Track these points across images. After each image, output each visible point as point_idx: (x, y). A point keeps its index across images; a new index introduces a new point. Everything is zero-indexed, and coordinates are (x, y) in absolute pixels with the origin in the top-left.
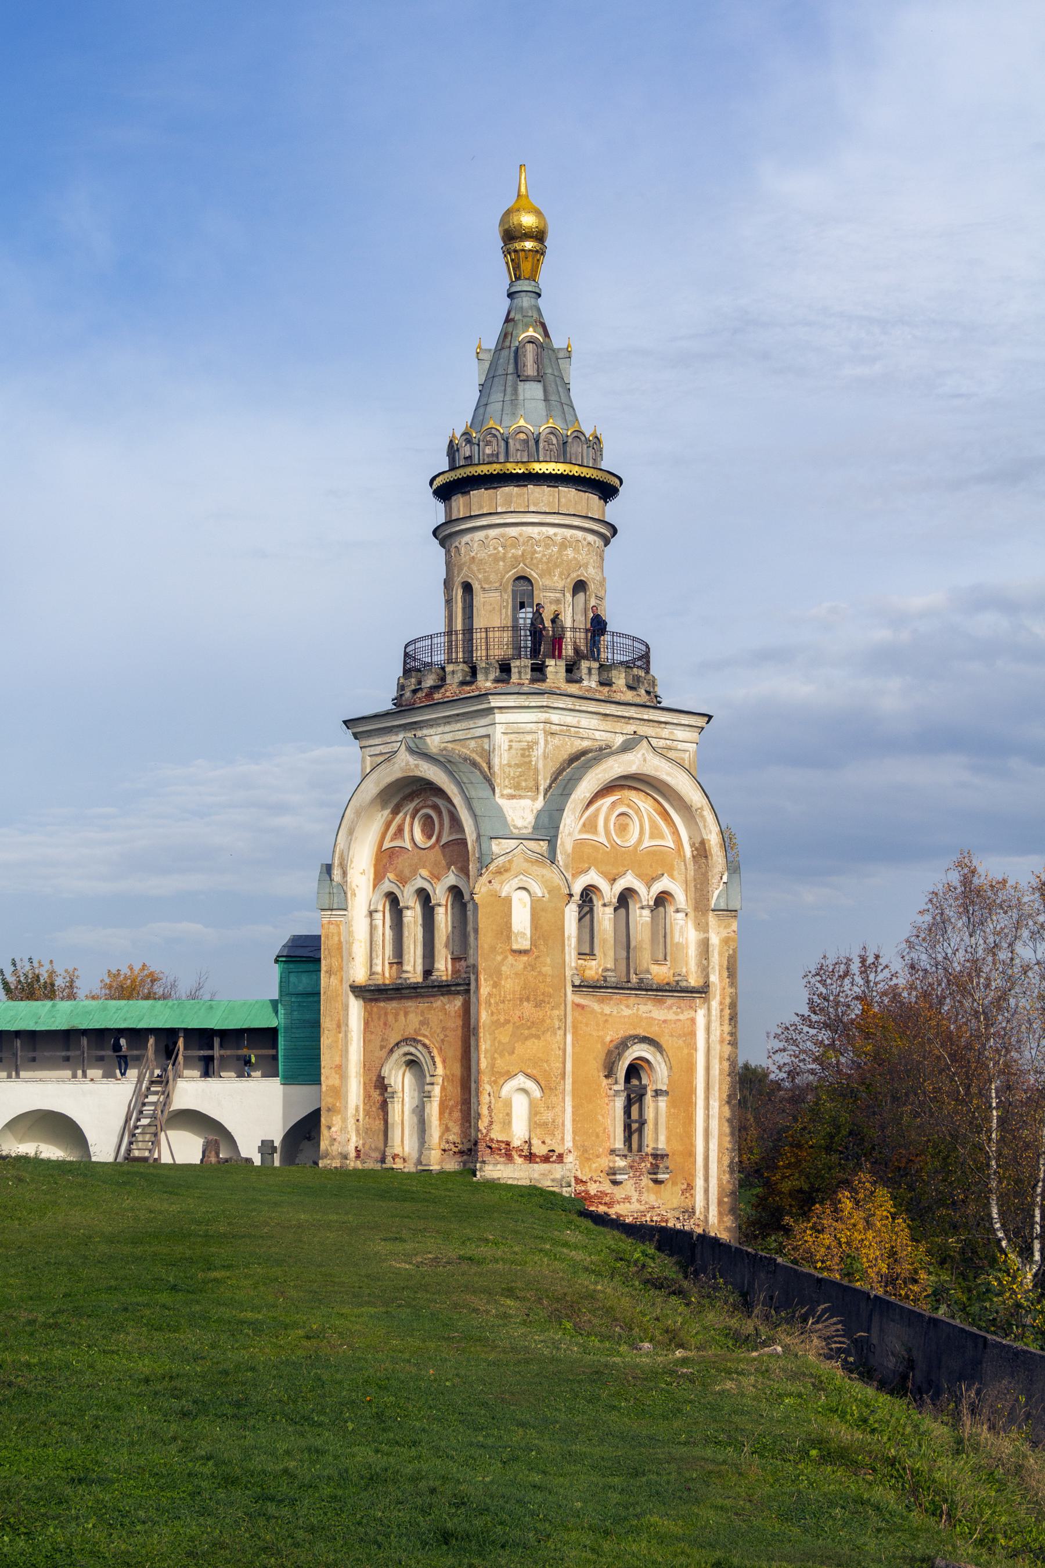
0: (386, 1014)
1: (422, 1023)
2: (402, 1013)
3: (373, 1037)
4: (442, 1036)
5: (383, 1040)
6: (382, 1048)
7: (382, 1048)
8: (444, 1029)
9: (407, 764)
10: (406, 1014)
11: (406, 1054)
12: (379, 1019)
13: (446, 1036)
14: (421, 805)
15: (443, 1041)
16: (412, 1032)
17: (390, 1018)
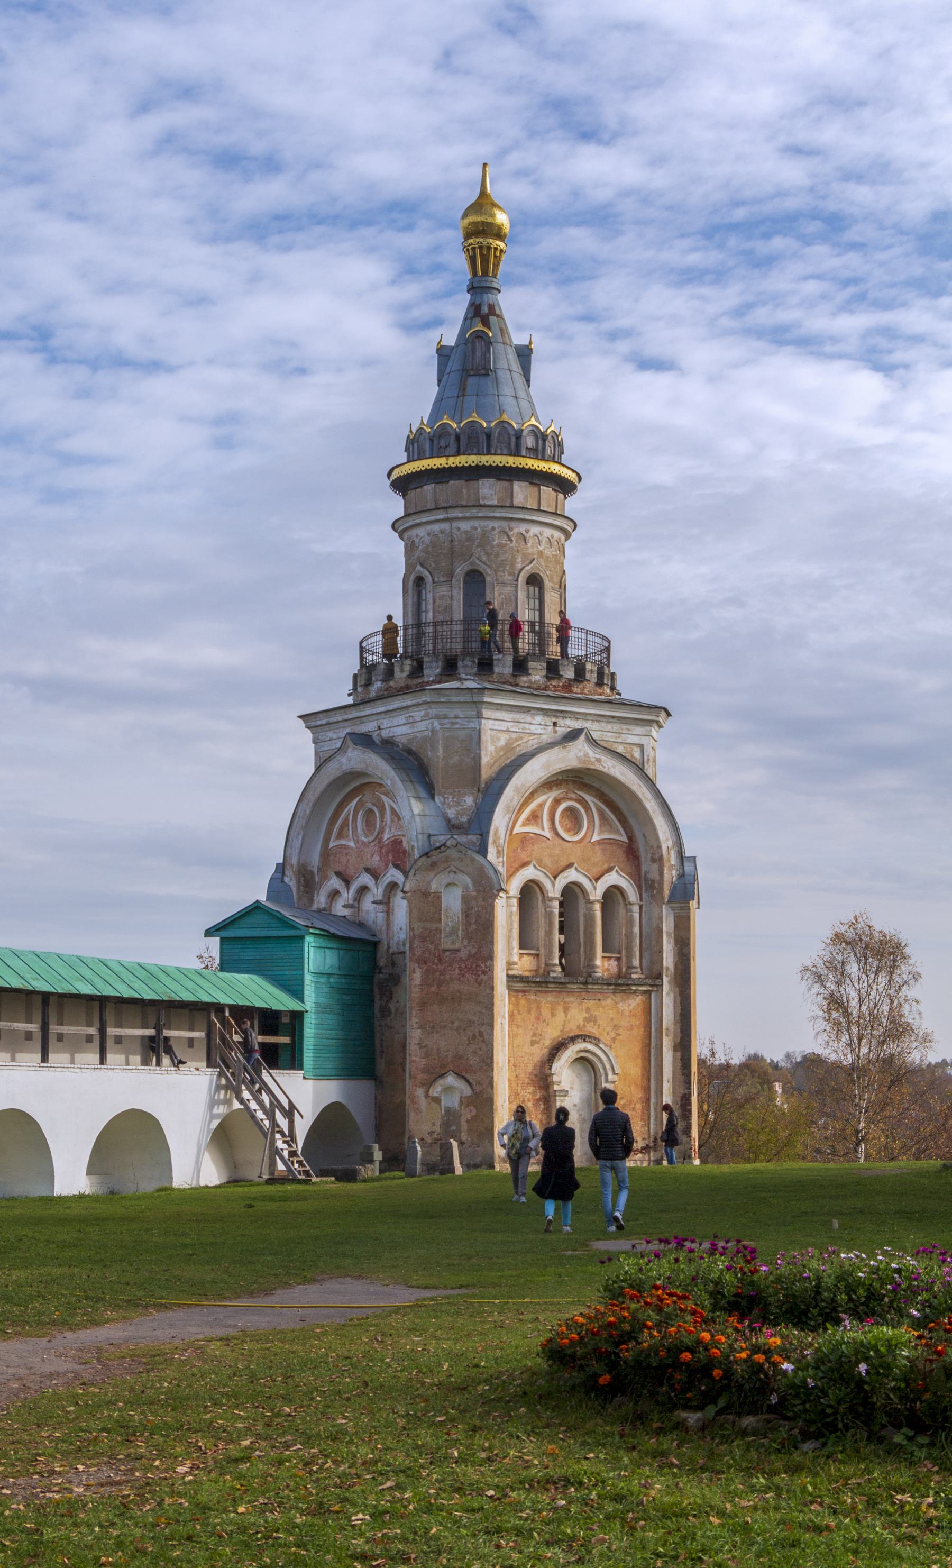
0: (539, 1008)
1: (587, 1020)
2: (561, 1008)
3: (521, 1031)
4: (613, 1035)
5: (534, 1035)
6: (533, 1043)
7: (533, 1043)
8: (616, 1027)
9: (586, 755)
10: (566, 1010)
11: (578, 1052)
12: (529, 1011)
13: (618, 1035)
14: (562, 796)
15: (614, 1039)
16: (574, 1028)
17: (546, 1013)
